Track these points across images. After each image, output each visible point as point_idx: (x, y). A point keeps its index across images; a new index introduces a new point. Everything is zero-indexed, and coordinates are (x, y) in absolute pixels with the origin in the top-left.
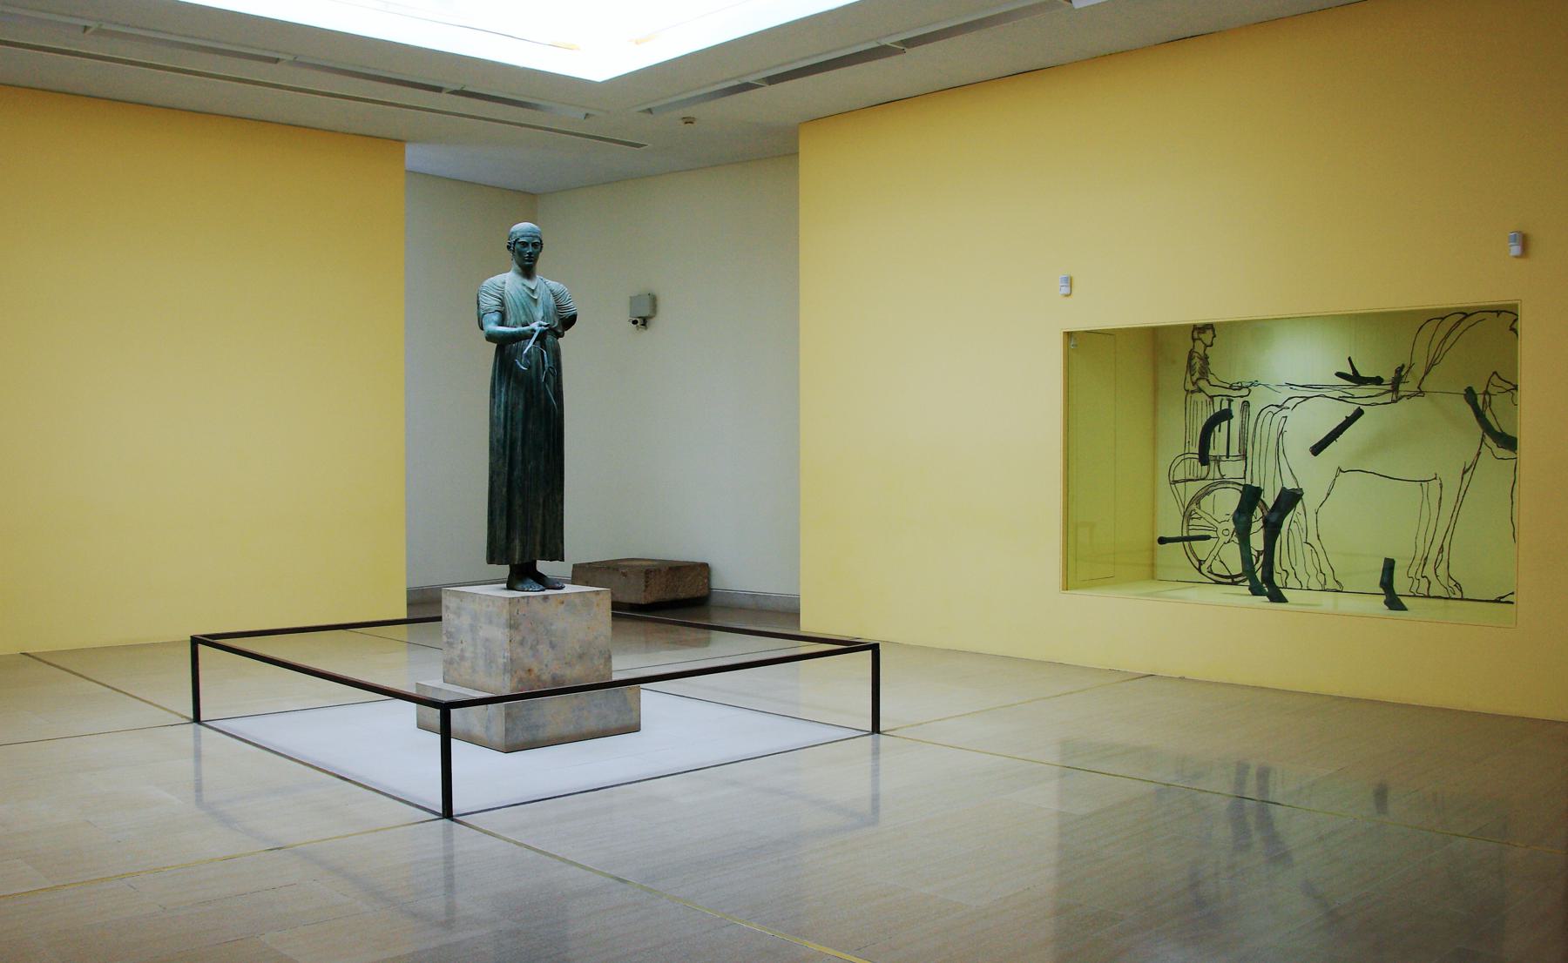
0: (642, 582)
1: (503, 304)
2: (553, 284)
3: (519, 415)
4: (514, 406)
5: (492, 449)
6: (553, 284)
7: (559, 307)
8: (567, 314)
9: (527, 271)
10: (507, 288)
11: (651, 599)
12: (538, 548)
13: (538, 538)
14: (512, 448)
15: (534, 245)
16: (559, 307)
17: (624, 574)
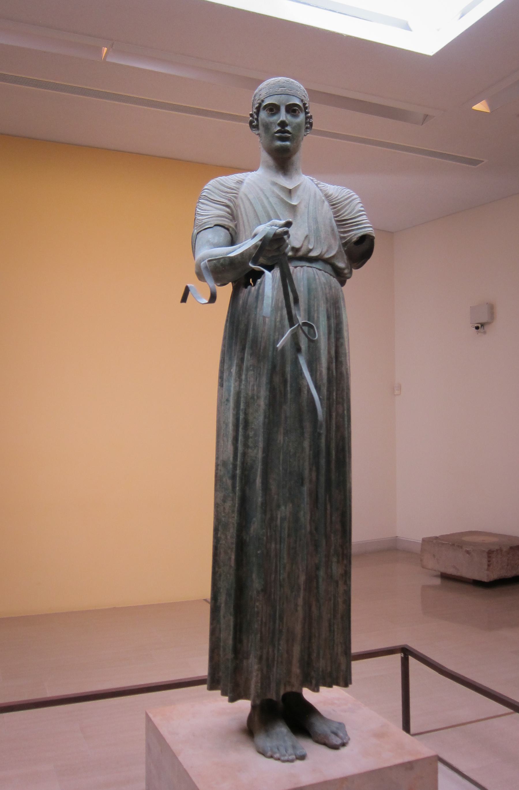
0: (485, 561)
1: (233, 216)
2: (333, 189)
3: (258, 419)
4: (251, 401)
5: (218, 479)
6: (333, 189)
7: (341, 223)
8: (356, 234)
9: (283, 160)
10: (244, 189)
11: (494, 576)
12: (296, 670)
13: (297, 650)
14: (246, 480)
15: (292, 109)
16: (341, 223)
17: (468, 552)
